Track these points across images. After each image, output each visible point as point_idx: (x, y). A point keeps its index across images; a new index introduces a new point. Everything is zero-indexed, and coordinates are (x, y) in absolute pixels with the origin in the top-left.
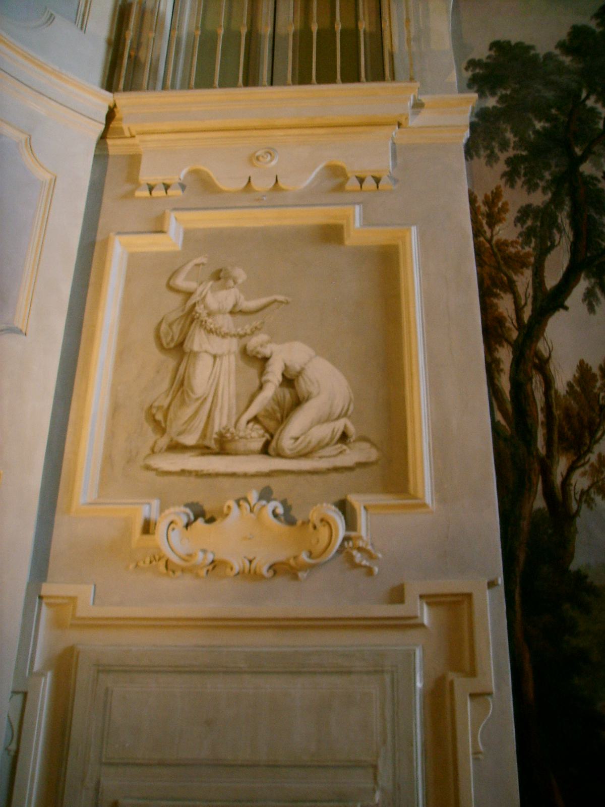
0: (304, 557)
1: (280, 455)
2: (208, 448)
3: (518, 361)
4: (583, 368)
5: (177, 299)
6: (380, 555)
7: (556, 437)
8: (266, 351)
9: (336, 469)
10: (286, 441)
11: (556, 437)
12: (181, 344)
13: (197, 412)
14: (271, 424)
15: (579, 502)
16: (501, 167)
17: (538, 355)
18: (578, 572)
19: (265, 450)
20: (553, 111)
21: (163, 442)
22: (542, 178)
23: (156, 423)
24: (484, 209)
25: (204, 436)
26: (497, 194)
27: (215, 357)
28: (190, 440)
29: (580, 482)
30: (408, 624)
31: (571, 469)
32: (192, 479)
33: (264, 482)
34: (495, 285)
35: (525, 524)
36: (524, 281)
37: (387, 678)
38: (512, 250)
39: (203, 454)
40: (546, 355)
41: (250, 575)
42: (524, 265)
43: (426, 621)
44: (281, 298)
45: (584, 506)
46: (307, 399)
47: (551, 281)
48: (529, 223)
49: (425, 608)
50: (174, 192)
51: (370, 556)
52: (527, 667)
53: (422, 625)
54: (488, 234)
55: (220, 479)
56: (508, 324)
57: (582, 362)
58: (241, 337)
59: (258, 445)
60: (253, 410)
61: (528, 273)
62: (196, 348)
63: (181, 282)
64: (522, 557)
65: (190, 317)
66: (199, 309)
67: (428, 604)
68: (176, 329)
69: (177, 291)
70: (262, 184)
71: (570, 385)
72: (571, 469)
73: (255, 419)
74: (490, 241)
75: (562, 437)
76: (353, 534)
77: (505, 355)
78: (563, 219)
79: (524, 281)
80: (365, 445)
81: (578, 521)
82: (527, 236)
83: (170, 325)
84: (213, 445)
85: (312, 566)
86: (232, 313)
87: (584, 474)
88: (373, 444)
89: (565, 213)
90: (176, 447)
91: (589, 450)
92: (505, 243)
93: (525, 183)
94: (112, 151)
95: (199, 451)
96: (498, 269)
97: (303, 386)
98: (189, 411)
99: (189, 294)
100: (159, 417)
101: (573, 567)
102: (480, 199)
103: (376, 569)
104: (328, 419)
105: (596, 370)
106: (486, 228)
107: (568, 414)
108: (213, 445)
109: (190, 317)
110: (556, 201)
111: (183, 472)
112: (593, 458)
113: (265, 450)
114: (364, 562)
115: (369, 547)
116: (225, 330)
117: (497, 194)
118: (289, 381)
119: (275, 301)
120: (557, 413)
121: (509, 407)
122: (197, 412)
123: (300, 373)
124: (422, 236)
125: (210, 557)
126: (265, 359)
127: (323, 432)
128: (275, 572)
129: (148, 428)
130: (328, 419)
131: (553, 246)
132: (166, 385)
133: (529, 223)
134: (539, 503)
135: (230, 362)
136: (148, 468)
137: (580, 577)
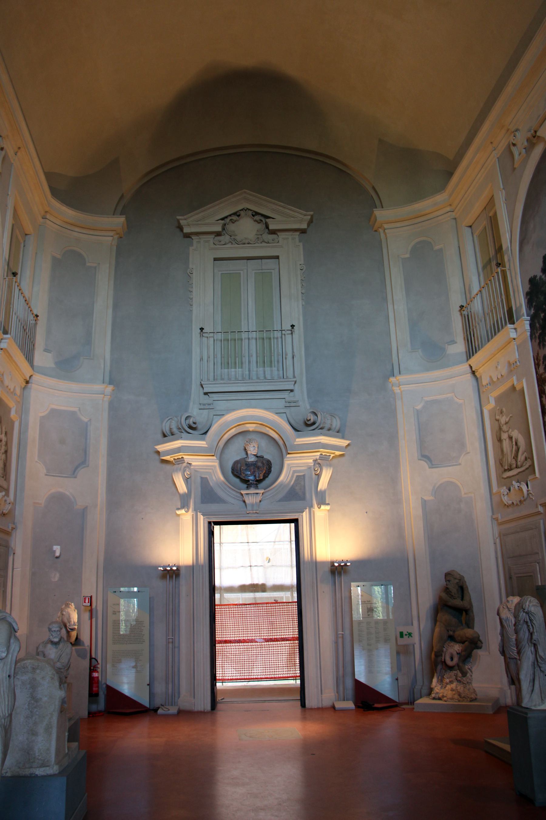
2: (509, 469)
5: (497, 422)
6: (533, 494)
9: (527, 469)
10: (519, 463)
14: (515, 457)
16: (537, 341)
19: (516, 467)
21: (503, 470)
25: (508, 467)
26: (538, 354)
28: (506, 468)
30: (539, 513)
32: (508, 479)
41: (517, 505)
43: (542, 512)
44: (511, 415)
49: (542, 508)
51: (532, 495)
53: (541, 513)
58: (508, 431)
59: (515, 466)
63: (497, 417)
65: (500, 429)
67: (542, 506)
70: (499, 377)
84: (509, 468)
86: (505, 424)
90: (505, 470)
92: (542, 375)
93: (542, 345)
94: (478, 376)
98: (505, 459)
103: (534, 499)
106: (538, 369)
108: (509, 468)
109: (500, 429)
114: (531, 497)
115: (532, 492)
116: (505, 430)
117: (538, 354)
123: (517, 440)
124: (527, 381)
126: (512, 437)
127: (523, 458)
128: (521, 503)
130: (523, 454)
135: (507, 440)
136: (503, 478)
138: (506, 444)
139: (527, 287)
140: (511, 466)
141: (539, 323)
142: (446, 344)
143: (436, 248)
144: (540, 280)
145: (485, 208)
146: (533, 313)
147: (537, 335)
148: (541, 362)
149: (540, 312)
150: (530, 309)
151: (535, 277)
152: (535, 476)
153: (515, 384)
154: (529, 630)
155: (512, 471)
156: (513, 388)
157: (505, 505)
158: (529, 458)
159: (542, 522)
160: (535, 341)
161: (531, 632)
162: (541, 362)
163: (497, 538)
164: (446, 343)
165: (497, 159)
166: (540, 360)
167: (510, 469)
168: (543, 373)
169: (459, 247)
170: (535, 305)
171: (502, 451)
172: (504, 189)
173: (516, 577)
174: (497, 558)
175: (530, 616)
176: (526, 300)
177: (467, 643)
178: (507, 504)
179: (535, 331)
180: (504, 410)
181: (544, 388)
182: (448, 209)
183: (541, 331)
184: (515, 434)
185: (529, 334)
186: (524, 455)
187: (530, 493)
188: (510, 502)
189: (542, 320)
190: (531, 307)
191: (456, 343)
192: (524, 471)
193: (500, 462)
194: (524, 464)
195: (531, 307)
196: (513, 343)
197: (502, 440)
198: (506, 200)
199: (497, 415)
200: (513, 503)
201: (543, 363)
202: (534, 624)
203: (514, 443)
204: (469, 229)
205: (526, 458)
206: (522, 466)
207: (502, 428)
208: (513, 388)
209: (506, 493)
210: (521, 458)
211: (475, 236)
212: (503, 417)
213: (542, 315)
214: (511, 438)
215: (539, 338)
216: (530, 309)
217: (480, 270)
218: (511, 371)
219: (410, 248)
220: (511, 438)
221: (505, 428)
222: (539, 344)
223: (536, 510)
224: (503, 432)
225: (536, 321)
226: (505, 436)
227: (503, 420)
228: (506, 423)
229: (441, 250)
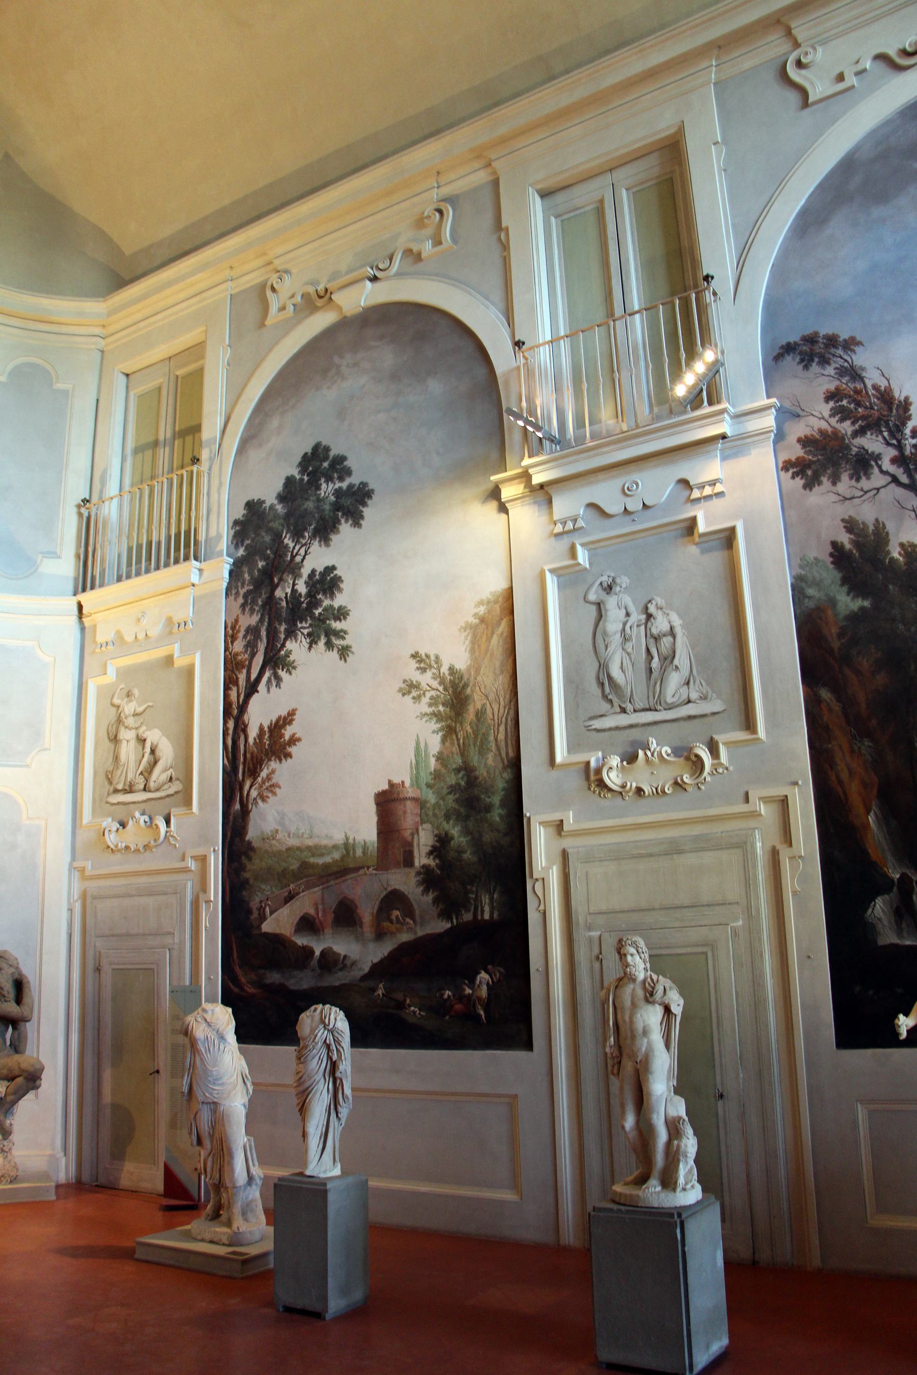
0: (152, 842)
1: (150, 791)
3: (236, 728)
4: (261, 728)
5: (114, 710)
7: (246, 770)
8: (145, 736)
9: (168, 796)
10: (152, 785)
11: (246, 770)
12: (116, 736)
13: (122, 772)
14: (146, 774)
15: (252, 805)
16: (241, 600)
17: (244, 723)
18: (249, 841)
19: (145, 790)
20: (268, 552)
21: (112, 789)
22: (257, 605)
23: (109, 779)
24: (230, 632)
25: (125, 784)
26: (237, 621)
27: (128, 741)
28: (120, 787)
29: (254, 793)
30: (186, 870)
31: (251, 787)
32: (122, 806)
33: (143, 806)
34: (230, 682)
35: (231, 818)
36: (242, 677)
37: (178, 895)
38: (240, 658)
39: (125, 793)
40: (247, 722)
41: (137, 851)
42: (243, 667)
43: (193, 869)
44: (150, 704)
45: (254, 806)
46: (159, 760)
47: (254, 676)
48: (248, 638)
50: (110, 647)
51: (176, 839)
52: (228, 887)
53: (191, 871)
54: (230, 650)
55: (131, 805)
56: (234, 706)
57: (261, 724)
58: (136, 728)
59: (142, 787)
60: (139, 772)
61: (245, 671)
62: (121, 738)
63: (116, 701)
64: (229, 834)
65: (119, 721)
66: (122, 715)
67: (195, 860)
68: (114, 727)
69: (113, 705)
70: (141, 636)
71: (255, 739)
72: (251, 787)
73: (141, 773)
74: (230, 654)
75: (249, 770)
76: (168, 829)
77: (231, 724)
78: (264, 633)
79: (242, 677)
80: (178, 782)
81: (251, 814)
82: (246, 646)
83: (112, 726)
84: (127, 788)
85: (156, 846)
86: (133, 715)
87: (255, 789)
88: (181, 782)
89: (264, 628)
90: (116, 791)
91: (259, 776)
92: (237, 654)
94: (87, 625)
95: (123, 792)
96: (233, 671)
97: (158, 753)
98: (119, 772)
99: (118, 707)
100: (110, 776)
101: (247, 838)
102: (230, 625)
104: (166, 770)
105: (266, 729)
107: (252, 754)
108: (127, 788)
109: (119, 721)
110: (261, 621)
111: (119, 803)
112: (260, 779)
113: (145, 790)
114: (173, 842)
115: (175, 835)
116: (131, 726)
117: (237, 621)
118: (153, 752)
119: (149, 706)
120: (248, 756)
121: (230, 755)
122: (122, 772)
123: (156, 746)
125: (124, 845)
126: (145, 740)
127: (164, 777)
129: (106, 783)
130: (166, 770)
131: (257, 651)
132: (111, 759)
133: (248, 638)
134: (237, 806)
135: (133, 743)
136: (107, 803)
137: (250, 843)
138: (128, 750)
139: (240, 513)
140: (131, 785)
141: (250, 574)
142: (40, 556)
143: (60, 386)
144: (269, 509)
145: (170, 358)
146: (242, 555)
147: (242, 592)
148: (241, 635)
149: (257, 558)
150: (237, 547)
151: (261, 502)
152: (191, 809)
153: (175, 656)
154: (329, 1058)
155: (133, 794)
156: (169, 660)
157: (109, 847)
158: (178, 779)
159: (189, 884)
160: (235, 599)
161: (334, 1060)
162: (241, 635)
163: (75, 902)
164: (41, 553)
165: (229, 296)
166: (239, 631)
167: (130, 790)
168: (241, 652)
169: (97, 400)
170: (248, 545)
171: (116, 758)
172: (230, 346)
173: (114, 969)
174: (70, 936)
175: (336, 1035)
176: (232, 532)
177: (20, 1080)
178: (112, 846)
179: (239, 584)
180: (136, 692)
181: (237, 676)
182: (97, 331)
183: (251, 588)
184: (153, 736)
185: (225, 585)
186: (169, 773)
187: (172, 836)
188: (122, 845)
189: (259, 570)
190: (240, 545)
191: (59, 557)
192: (160, 798)
193: (107, 776)
194: (164, 788)
195: (240, 545)
196: (191, 590)
197: (121, 741)
198: (229, 364)
199: (116, 696)
200: (127, 848)
201: (245, 637)
202: (343, 1048)
203: (148, 750)
204: (124, 378)
205: (171, 778)
206: (158, 790)
207: (124, 720)
208: (169, 660)
209: (116, 829)
210: (159, 775)
211: (132, 394)
212: (130, 704)
213: (261, 564)
214: (142, 741)
215: (245, 597)
216: (237, 547)
217: (129, 451)
218: (171, 633)
219: (10, 367)
220: (142, 741)
221: (131, 721)
222: (243, 606)
223: (182, 865)
224: (126, 727)
225: (245, 569)
226: (127, 735)
227: (129, 708)
228: (136, 715)
229: (65, 393)
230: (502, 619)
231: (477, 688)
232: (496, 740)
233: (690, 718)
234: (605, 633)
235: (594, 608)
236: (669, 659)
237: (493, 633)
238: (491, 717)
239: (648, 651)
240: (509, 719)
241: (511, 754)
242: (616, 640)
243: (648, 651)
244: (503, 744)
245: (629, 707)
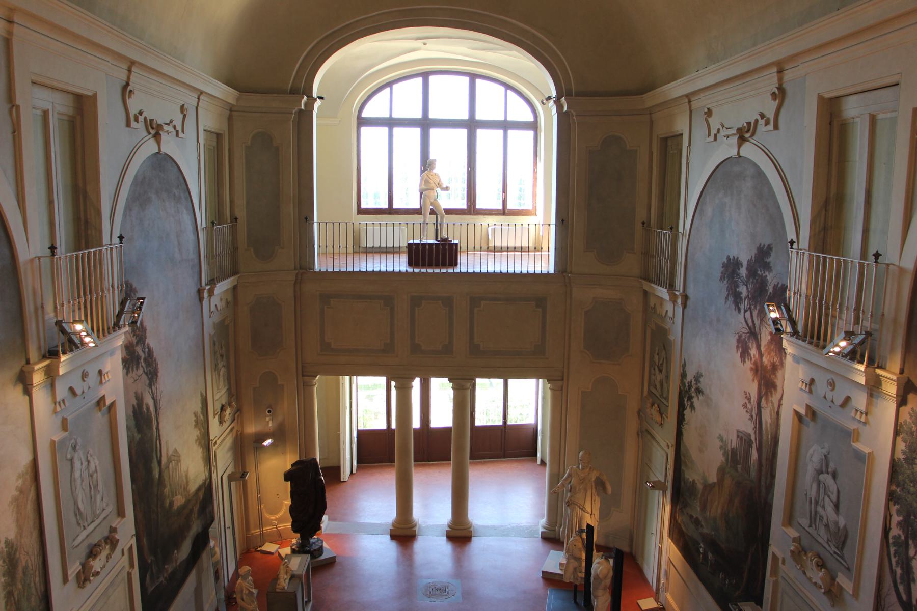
230: (31, 487)
231: (22, 549)
232: (35, 583)
233: (105, 518)
234: (74, 478)
235: (70, 463)
236: (96, 486)
237: (27, 500)
238: (31, 568)
239: (90, 484)
240: (40, 563)
241: (43, 589)
242: (79, 481)
243: (90, 484)
244: (38, 584)
245: (86, 524)
